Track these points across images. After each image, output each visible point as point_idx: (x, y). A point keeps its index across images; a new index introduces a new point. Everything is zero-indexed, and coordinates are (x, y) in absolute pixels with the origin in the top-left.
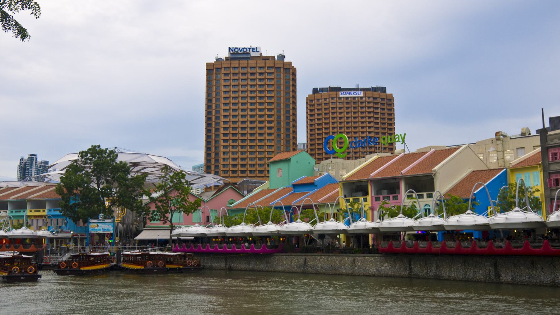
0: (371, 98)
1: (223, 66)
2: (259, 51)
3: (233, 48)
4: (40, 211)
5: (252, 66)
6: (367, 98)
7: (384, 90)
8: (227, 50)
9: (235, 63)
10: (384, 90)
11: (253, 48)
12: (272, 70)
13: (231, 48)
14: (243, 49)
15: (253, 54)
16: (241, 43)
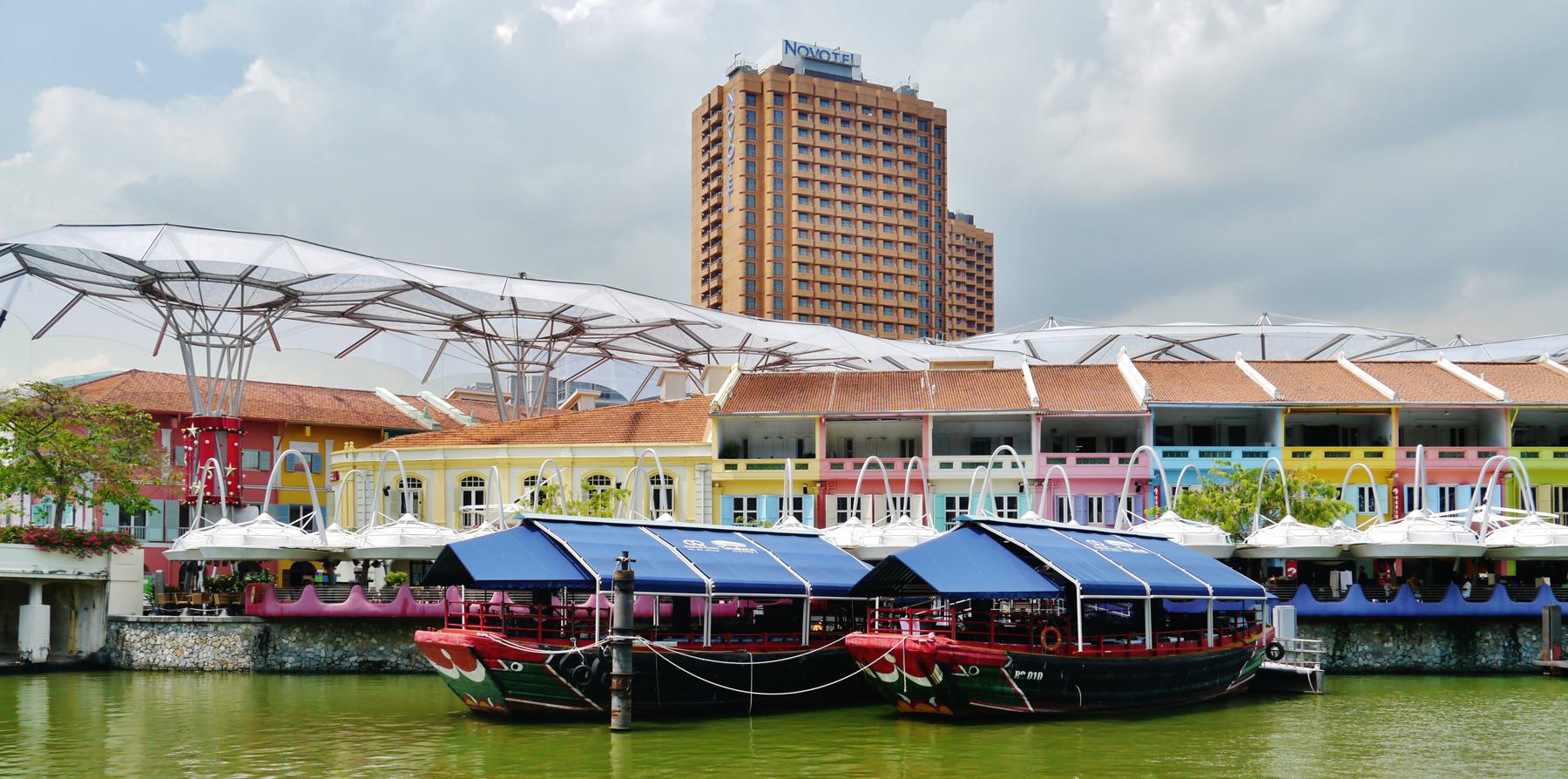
0: (962, 237)
1: (793, 90)
2: (858, 67)
3: (795, 43)
4: (1106, 461)
5: (867, 104)
6: (954, 236)
7: (970, 219)
8: (780, 47)
9: (826, 88)
10: (970, 219)
11: (844, 56)
12: (914, 125)
13: (791, 40)
14: (820, 52)
15: (855, 76)
16: (827, 38)
